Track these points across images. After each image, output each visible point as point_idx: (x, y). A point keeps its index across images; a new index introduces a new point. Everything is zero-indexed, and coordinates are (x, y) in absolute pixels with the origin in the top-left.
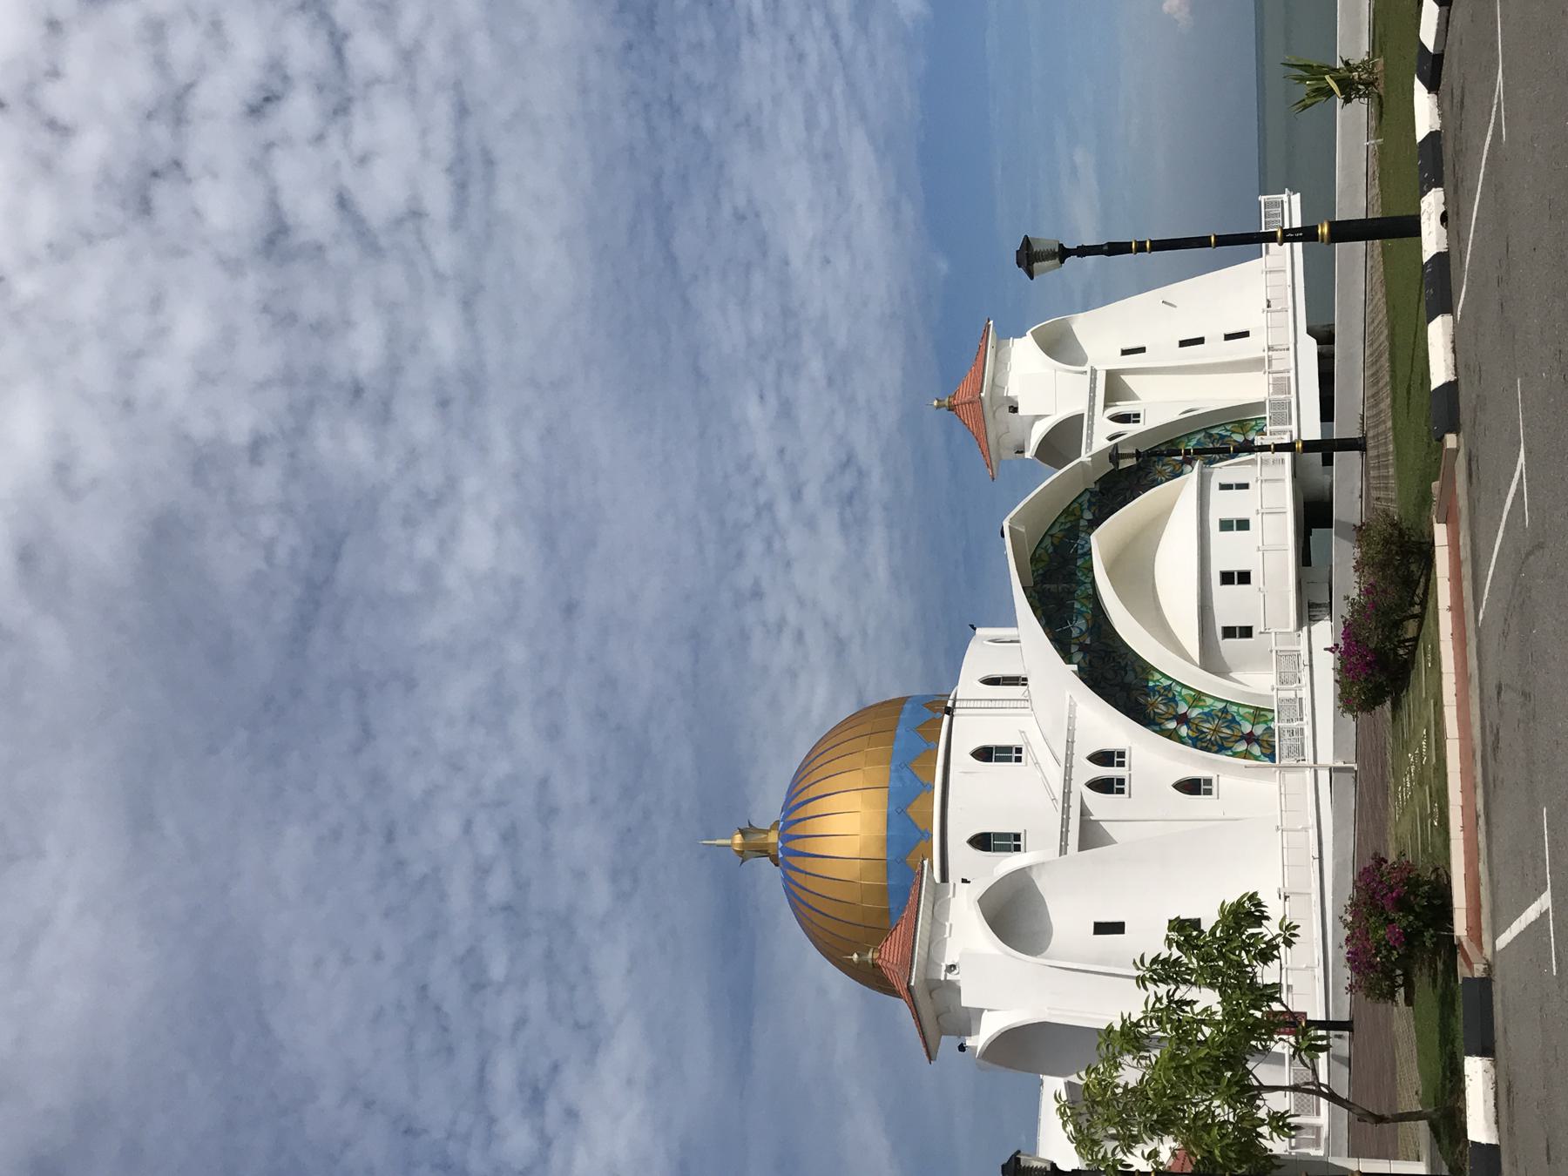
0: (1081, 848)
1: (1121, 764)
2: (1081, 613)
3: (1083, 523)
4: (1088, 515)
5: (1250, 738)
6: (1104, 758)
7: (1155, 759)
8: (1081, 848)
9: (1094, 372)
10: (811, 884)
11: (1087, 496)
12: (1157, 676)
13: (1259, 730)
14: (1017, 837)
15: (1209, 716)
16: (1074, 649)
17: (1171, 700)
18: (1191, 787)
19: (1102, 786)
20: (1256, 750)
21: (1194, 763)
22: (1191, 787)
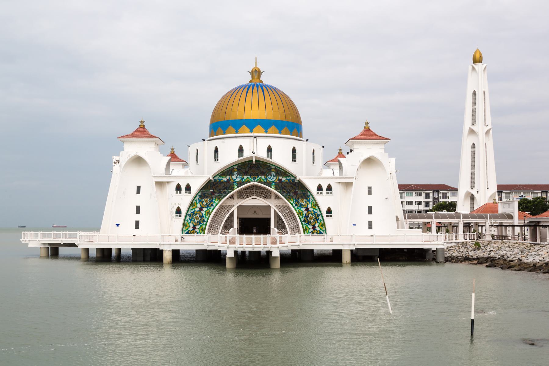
0: (156, 182)
1: (186, 193)
2: (242, 179)
3: (280, 178)
4: (284, 179)
5: (194, 228)
6: (188, 188)
7: (184, 201)
8: (156, 182)
9: (352, 178)
10: (239, 95)
11: (292, 178)
12: (217, 202)
13: (197, 230)
14: (218, 160)
15: (202, 216)
16: (228, 177)
17: (207, 206)
18: (178, 211)
19: (178, 188)
20: (191, 229)
21: (183, 213)
22: (178, 211)
